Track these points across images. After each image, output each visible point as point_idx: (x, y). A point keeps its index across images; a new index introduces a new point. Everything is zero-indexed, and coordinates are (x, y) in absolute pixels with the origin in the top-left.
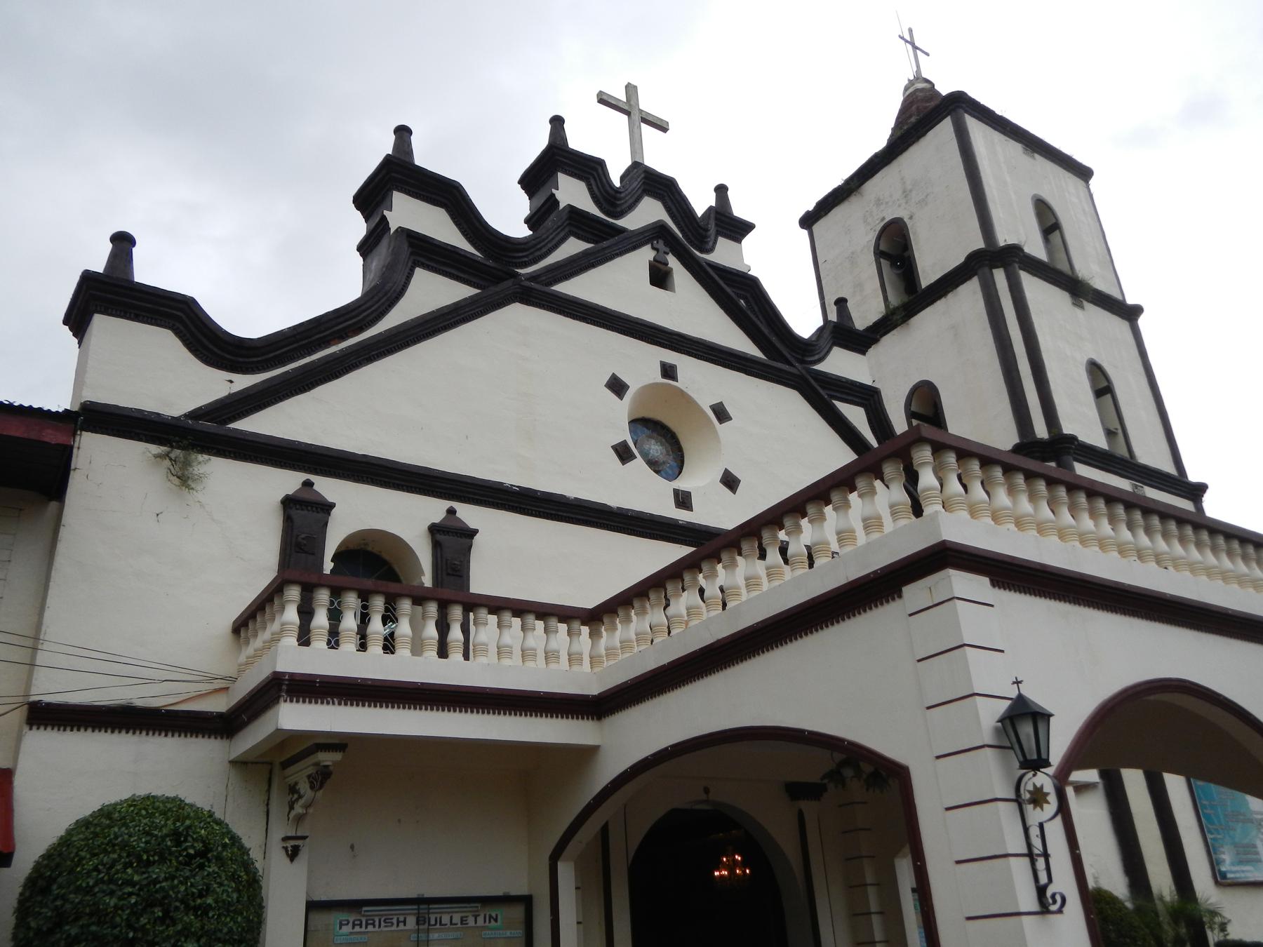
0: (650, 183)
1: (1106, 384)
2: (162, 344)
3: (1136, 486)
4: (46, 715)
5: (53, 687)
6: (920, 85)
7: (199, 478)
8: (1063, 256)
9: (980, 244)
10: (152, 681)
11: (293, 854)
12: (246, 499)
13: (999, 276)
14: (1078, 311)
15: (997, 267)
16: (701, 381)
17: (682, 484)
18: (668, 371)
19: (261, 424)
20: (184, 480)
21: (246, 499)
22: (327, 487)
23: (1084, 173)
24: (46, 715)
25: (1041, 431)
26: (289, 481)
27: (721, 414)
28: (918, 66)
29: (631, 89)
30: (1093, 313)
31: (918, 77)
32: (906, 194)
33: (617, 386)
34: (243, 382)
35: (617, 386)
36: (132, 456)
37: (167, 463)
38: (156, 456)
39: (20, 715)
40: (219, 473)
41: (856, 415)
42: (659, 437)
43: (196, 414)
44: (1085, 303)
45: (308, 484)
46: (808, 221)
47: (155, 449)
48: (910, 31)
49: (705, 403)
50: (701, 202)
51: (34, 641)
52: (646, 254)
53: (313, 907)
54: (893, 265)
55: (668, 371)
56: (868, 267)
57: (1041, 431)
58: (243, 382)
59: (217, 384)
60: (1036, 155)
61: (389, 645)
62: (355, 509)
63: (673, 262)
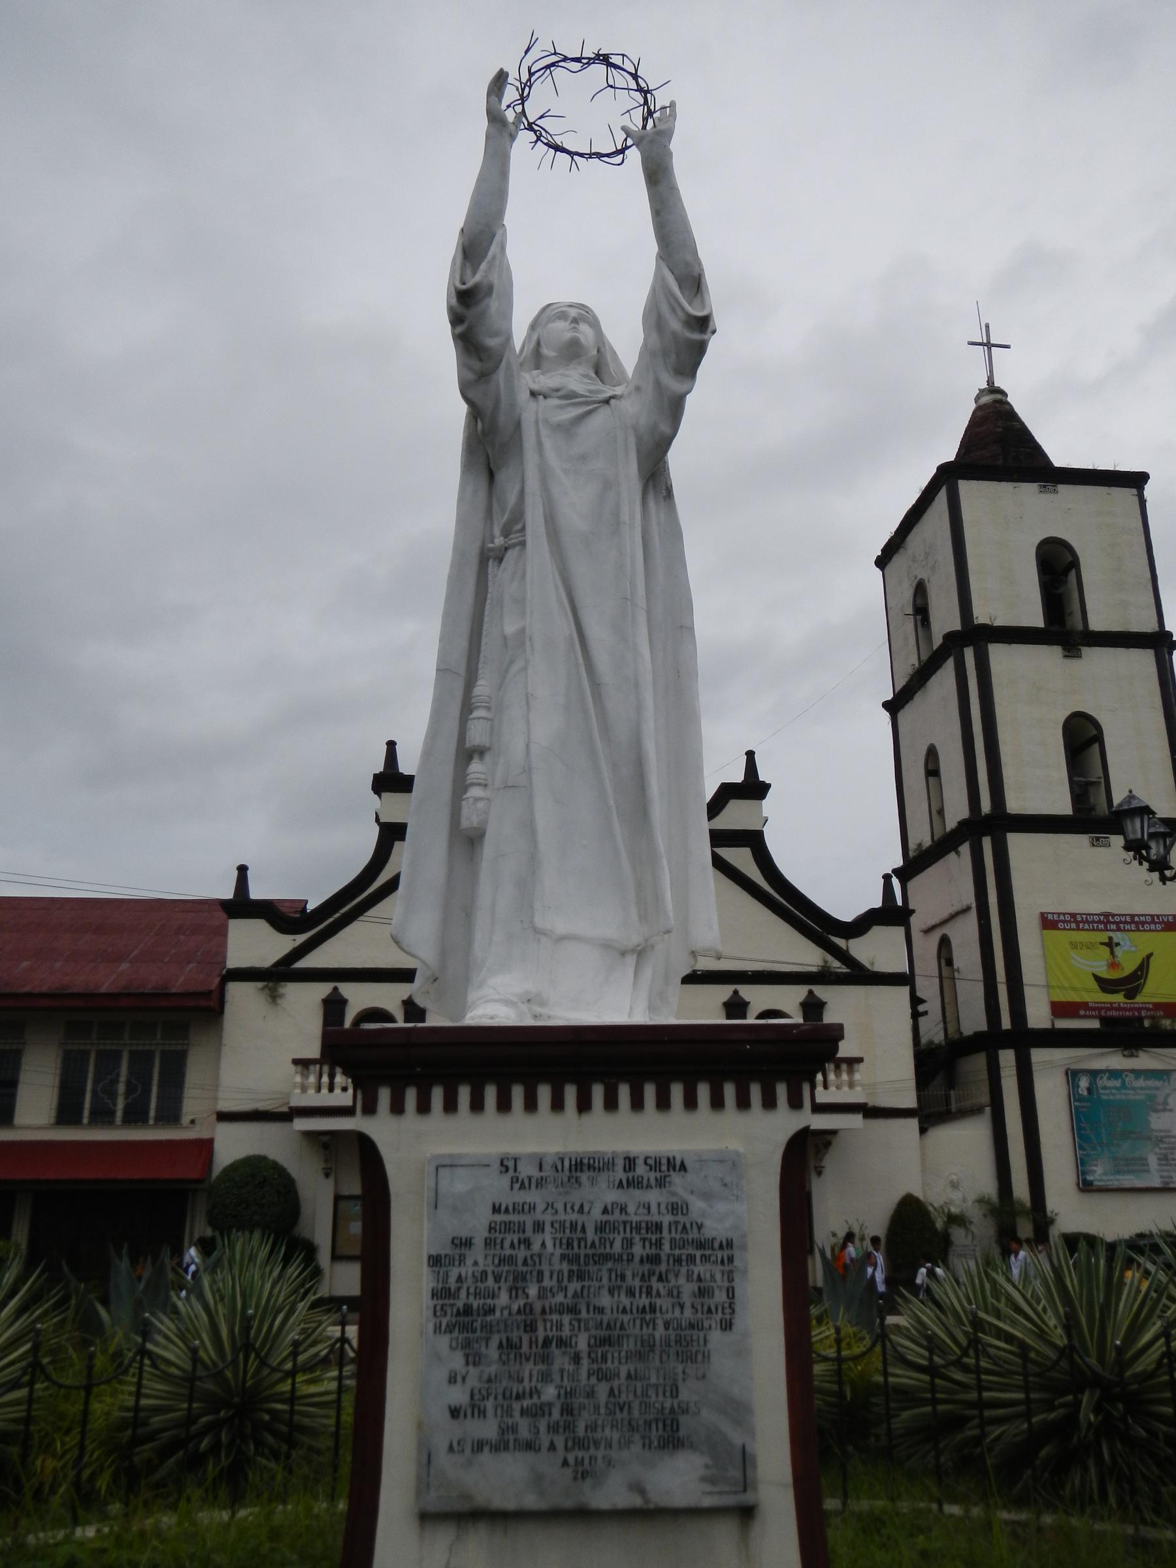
1: (1095, 732)
3: (1098, 839)
4: (225, 1117)
5: (226, 1106)
6: (986, 399)
7: (282, 996)
8: (1076, 595)
9: (957, 626)
10: (261, 1100)
11: (327, 1175)
12: (304, 1001)
13: (969, 654)
14: (1073, 663)
15: (967, 646)
19: (310, 961)
21: (304, 1001)
23: (1137, 481)
24: (225, 1117)
25: (986, 806)
26: (323, 989)
28: (991, 371)
30: (1096, 659)
31: (992, 389)
32: (927, 555)
34: (301, 938)
37: (267, 991)
38: (262, 989)
39: (214, 1117)
45: (336, 989)
47: (260, 985)
48: (987, 326)
51: (216, 1086)
53: (338, 1198)
54: (923, 625)
56: (910, 625)
57: (986, 806)
58: (301, 938)
59: (285, 944)
60: (1060, 487)
62: (360, 997)
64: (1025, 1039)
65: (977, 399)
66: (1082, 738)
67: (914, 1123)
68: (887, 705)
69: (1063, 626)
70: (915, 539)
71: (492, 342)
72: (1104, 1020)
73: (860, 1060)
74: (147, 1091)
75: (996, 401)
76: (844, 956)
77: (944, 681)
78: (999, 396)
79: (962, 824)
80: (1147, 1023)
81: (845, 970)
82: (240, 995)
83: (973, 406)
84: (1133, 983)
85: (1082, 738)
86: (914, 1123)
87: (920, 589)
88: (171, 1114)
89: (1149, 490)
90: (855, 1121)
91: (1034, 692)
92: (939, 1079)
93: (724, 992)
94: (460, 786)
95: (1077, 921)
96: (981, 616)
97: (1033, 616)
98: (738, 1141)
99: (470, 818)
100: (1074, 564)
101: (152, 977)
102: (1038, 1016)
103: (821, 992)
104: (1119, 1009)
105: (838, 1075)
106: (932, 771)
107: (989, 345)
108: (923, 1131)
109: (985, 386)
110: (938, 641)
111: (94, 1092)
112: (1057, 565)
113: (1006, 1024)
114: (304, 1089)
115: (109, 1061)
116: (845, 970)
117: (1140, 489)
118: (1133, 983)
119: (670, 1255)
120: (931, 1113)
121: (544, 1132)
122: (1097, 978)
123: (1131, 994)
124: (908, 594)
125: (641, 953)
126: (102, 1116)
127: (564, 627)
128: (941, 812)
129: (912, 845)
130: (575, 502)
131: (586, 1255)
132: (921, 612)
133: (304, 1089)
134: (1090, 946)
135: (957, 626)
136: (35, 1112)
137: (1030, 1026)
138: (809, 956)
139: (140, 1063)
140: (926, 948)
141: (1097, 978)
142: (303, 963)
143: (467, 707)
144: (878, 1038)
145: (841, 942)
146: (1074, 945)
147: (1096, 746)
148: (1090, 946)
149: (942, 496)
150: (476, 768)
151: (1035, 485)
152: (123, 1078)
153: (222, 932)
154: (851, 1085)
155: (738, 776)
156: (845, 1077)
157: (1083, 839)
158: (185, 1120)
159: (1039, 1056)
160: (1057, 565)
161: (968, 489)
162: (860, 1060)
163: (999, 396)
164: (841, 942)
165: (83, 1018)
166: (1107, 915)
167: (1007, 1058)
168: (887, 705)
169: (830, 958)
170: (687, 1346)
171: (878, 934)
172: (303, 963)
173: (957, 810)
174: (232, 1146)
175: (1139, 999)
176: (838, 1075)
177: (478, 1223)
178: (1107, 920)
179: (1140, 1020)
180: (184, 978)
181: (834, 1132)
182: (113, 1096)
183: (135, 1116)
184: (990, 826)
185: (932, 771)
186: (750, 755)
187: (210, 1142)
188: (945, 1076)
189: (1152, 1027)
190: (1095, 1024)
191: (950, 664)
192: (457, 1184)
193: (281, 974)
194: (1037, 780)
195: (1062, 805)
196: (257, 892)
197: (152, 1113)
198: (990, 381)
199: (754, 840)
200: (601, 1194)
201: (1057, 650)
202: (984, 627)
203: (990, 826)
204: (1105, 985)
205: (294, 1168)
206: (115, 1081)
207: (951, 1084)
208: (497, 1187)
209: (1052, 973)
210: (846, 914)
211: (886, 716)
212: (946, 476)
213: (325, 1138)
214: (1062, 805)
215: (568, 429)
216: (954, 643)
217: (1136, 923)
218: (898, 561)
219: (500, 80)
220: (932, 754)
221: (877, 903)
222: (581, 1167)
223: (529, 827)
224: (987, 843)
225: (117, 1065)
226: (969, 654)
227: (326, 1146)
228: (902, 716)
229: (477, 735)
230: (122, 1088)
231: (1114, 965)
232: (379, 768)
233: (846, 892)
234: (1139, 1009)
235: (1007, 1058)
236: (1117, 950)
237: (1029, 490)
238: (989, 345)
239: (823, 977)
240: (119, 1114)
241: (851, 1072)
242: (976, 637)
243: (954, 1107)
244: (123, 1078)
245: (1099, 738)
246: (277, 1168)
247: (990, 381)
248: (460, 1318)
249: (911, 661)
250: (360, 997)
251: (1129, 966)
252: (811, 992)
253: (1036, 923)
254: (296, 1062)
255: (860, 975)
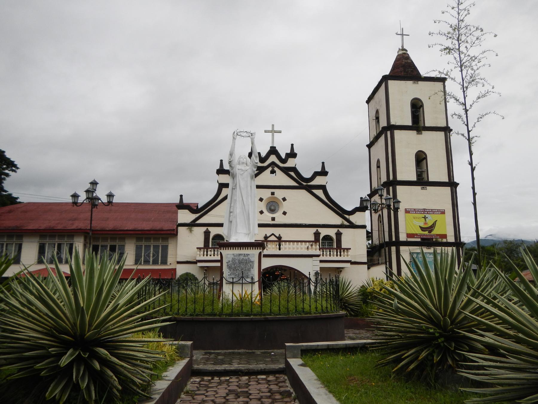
0: (273, 151)
2: (187, 211)
4: (179, 263)
5: (179, 260)
6: (401, 52)
9: (386, 125)
12: (199, 232)
13: (389, 133)
16: (279, 194)
17: (273, 216)
18: (273, 194)
20: (191, 231)
21: (199, 232)
22: (210, 229)
23: (443, 80)
24: (179, 263)
25: (391, 178)
26: (204, 229)
27: (284, 199)
29: (273, 126)
30: (426, 134)
33: (261, 200)
34: (198, 215)
35: (261, 200)
36: (185, 228)
40: (195, 229)
41: (319, 193)
42: (273, 206)
43: (192, 222)
44: (423, 132)
46: (368, 102)
47: (187, 227)
49: (280, 198)
50: (283, 152)
51: (176, 255)
52: (270, 169)
55: (273, 194)
56: (374, 123)
57: (391, 178)
58: (198, 215)
59: (194, 216)
60: (419, 82)
61: (207, 255)
62: (214, 231)
63: (276, 169)
64: (399, 244)
65: (398, 52)
66: (421, 159)
67: (366, 266)
68: (368, 146)
69: (417, 124)
70: (376, 96)
71: (233, 166)
72: (421, 239)
73: (350, 249)
74: (158, 256)
75: (403, 53)
76: (348, 220)
77: (382, 139)
78: (404, 52)
79: (384, 183)
80: (434, 240)
81: (348, 224)
82: (182, 230)
83: (397, 54)
84: (431, 229)
85: (421, 159)
86: (366, 266)
87: (377, 112)
88: (164, 262)
89: (447, 83)
90: (348, 265)
91: (407, 144)
92: (377, 254)
93: (314, 230)
94: (230, 216)
95: (416, 211)
96: (393, 122)
97: (409, 122)
98: (254, 253)
99: (231, 220)
100: (422, 106)
101: (158, 225)
102: (403, 237)
103: (341, 230)
104: (426, 236)
105: (344, 253)
106: (378, 167)
107: (402, 35)
108: (369, 268)
109: (401, 48)
110: (381, 129)
111: (144, 256)
112: (417, 106)
113: (394, 239)
114: (200, 256)
115: (148, 247)
116: (348, 224)
117: (444, 82)
118: (431, 229)
119: (248, 262)
120: (371, 263)
121: (237, 251)
122: (421, 228)
123: (430, 232)
124: (375, 113)
125: (249, 234)
126: (147, 262)
127: (241, 199)
128: (380, 178)
129: (373, 188)
130: (242, 184)
131: (240, 262)
132: (377, 118)
133: (200, 256)
134: (419, 218)
135: (386, 125)
136: (129, 262)
137: (400, 240)
138: (338, 220)
139: (156, 247)
140: (375, 216)
141: (421, 228)
142: (199, 222)
143: (230, 207)
144: (356, 243)
145: (347, 216)
146: (414, 218)
147: (425, 160)
148: (419, 218)
149: (383, 85)
150: (231, 214)
151: (411, 82)
152: (152, 253)
153: (177, 213)
154: (347, 256)
155: (319, 169)
156: (346, 253)
157: (419, 188)
158: (168, 263)
159: (402, 248)
160: (417, 106)
161: (391, 83)
162: (350, 249)
163: (404, 52)
164: (347, 216)
165: (140, 235)
166: (424, 209)
167: (393, 249)
168: (368, 146)
169: (344, 221)
170: (249, 270)
171: (358, 213)
172: (199, 222)
173: (384, 179)
174: (181, 270)
175: (432, 233)
176: (344, 253)
177: (231, 260)
178: (424, 211)
179: (432, 239)
180: (167, 226)
181: (343, 268)
182: (149, 257)
183: (155, 262)
184: (392, 183)
185: (378, 167)
186: (323, 163)
187: (176, 269)
188: (376, 254)
189: (436, 241)
190: (419, 240)
191: (383, 136)
192: (229, 256)
193: (193, 224)
194: (406, 170)
195: (414, 178)
196: (185, 201)
197: (160, 262)
198: (403, 47)
199: (323, 188)
200: (242, 257)
201: (415, 132)
202: (393, 125)
203: (392, 183)
204: (423, 229)
205: (197, 276)
206: (150, 253)
207: (380, 255)
208: (232, 256)
209: (408, 225)
210: (349, 208)
211: (367, 149)
212: (385, 79)
213: (206, 268)
214: (414, 178)
215: (242, 175)
216: (384, 130)
217: (433, 212)
218: (372, 102)
219: (234, 133)
220: (378, 161)
221: (358, 205)
222: (240, 255)
223: (237, 222)
224: (391, 188)
225: (150, 249)
226: (389, 133)
227: (206, 270)
228: (371, 149)
229: (231, 211)
230: (151, 255)
231: (426, 223)
232: (218, 167)
233: (349, 204)
234: (432, 236)
235: (393, 249)
236: (427, 219)
237: (409, 84)
238: (402, 35)
239: (342, 226)
240: (151, 262)
241: (347, 252)
242: (391, 128)
243: (380, 262)
244: (152, 253)
245: (426, 158)
246: (193, 276)
247: (403, 47)
248: (229, 267)
249: (374, 133)
250: (214, 231)
251: (430, 224)
252: (338, 230)
253: (404, 211)
254: (197, 248)
255: (352, 226)
